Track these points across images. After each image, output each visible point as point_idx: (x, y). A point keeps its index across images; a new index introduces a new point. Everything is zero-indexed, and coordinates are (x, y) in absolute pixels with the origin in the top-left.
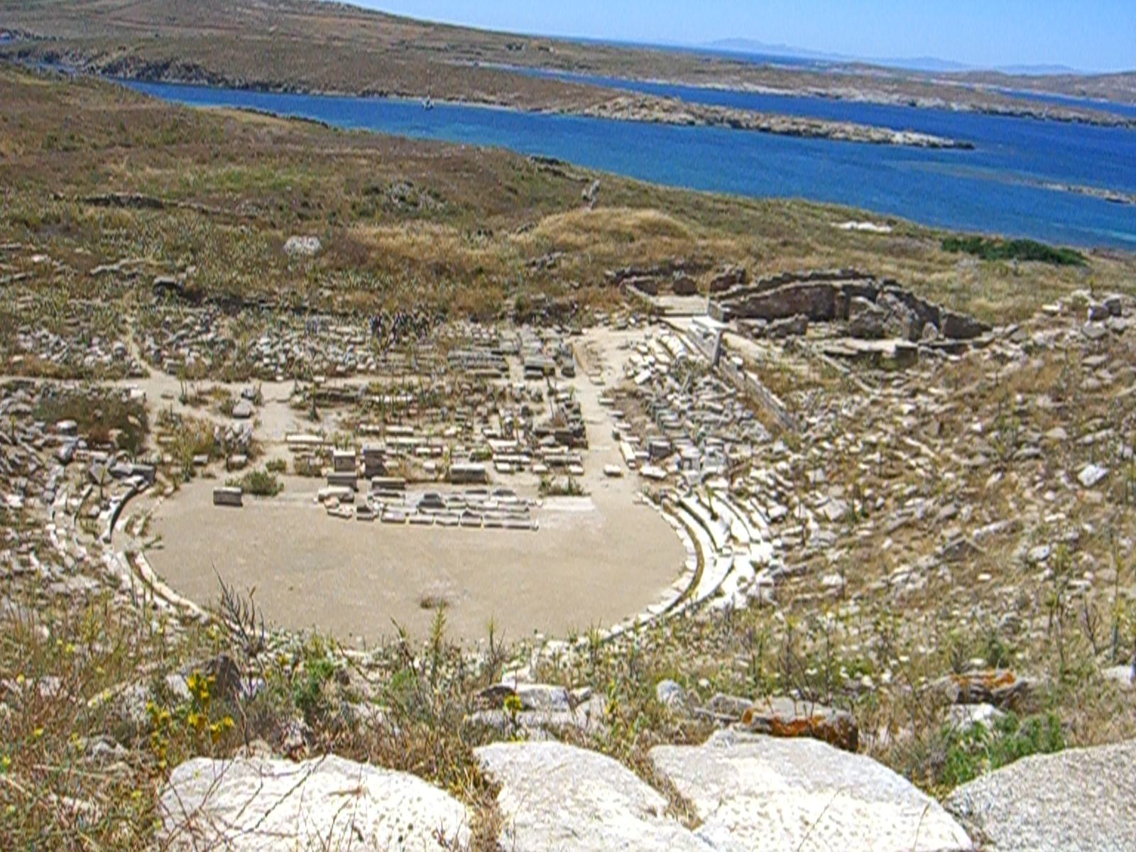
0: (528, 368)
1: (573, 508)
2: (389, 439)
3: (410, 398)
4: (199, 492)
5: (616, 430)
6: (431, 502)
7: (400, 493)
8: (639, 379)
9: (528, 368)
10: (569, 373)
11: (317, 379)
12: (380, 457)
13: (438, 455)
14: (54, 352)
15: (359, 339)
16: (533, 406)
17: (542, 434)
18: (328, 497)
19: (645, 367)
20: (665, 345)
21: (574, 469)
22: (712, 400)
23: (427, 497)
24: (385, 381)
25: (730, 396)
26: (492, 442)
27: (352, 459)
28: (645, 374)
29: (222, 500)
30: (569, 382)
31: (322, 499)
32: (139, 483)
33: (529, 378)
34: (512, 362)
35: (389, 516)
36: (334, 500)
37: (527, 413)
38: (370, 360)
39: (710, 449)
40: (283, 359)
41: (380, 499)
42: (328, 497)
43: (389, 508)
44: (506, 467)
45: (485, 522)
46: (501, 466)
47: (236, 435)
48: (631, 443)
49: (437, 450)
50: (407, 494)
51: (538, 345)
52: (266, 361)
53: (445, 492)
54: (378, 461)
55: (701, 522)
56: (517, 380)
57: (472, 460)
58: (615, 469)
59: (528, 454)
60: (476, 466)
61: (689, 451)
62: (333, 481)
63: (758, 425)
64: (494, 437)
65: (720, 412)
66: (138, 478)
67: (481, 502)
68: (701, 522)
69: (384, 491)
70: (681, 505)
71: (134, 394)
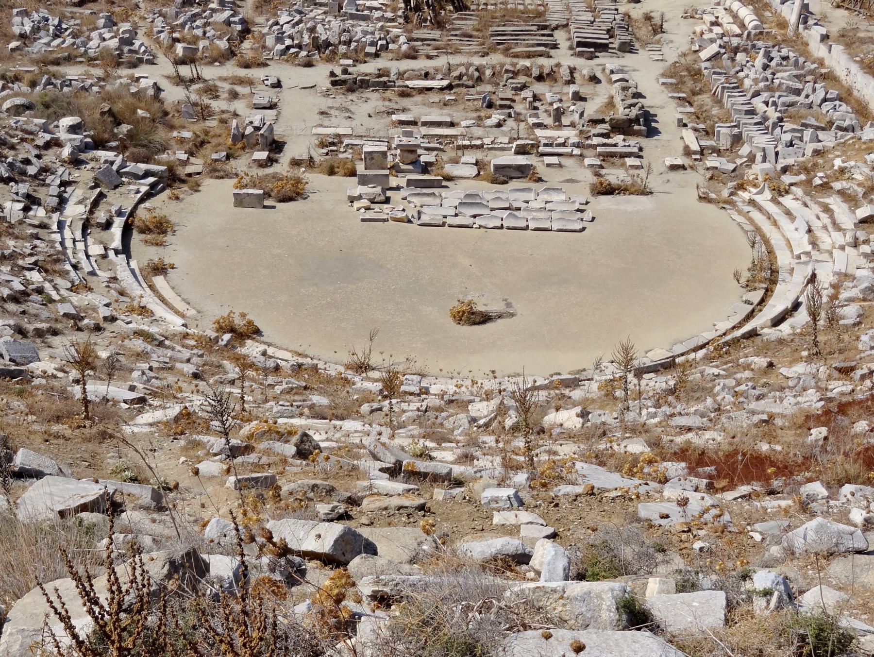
0: (579, 44)
1: (630, 208)
2: (424, 130)
3: (445, 83)
4: (217, 193)
5: (680, 116)
6: (471, 200)
7: (436, 191)
8: (704, 55)
9: (579, 44)
10: (627, 48)
11: (342, 62)
12: (413, 152)
13: (481, 147)
14: (56, 36)
15: (389, 15)
16: (584, 91)
17: (595, 122)
18: (360, 197)
19: (712, 41)
20: (735, 17)
21: (630, 161)
22: (790, 78)
23: (468, 196)
24: (421, 64)
25: (812, 72)
26: (539, 132)
27: (384, 154)
28: (714, 48)
29: (240, 201)
30: (628, 60)
31: (352, 199)
32: (153, 186)
33: (580, 55)
34: (560, 36)
35: (425, 219)
36: (365, 202)
37: (578, 97)
38: (402, 39)
39: (787, 137)
40: (306, 39)
41: (415, 199)
42: (360, 197)
43: (424, 209)
44: (554, 160)
45: (532, 225)
46: (548, 160)
47: (257, 129)
48: (696, 130)
49: (479, 142)
50: (444, 192)
51: (589, 17)
52: (288, 42)
53: (487, 191)
54: (412, 157)
55: (775, 223)
56: (564, 58)
57: (517, 153)
58: (679, 161)
59: (577, 145)
60: (522, 160)
61: (761, 140)
62: (364, 181)
63: (844, 107)
64: (539, 125)
65: (798, 92)
66: (151, 180)
67: (527, 202)
68: (775, 223)
69: (419, 190)
70: (752, 202)
71: (143, 83)
